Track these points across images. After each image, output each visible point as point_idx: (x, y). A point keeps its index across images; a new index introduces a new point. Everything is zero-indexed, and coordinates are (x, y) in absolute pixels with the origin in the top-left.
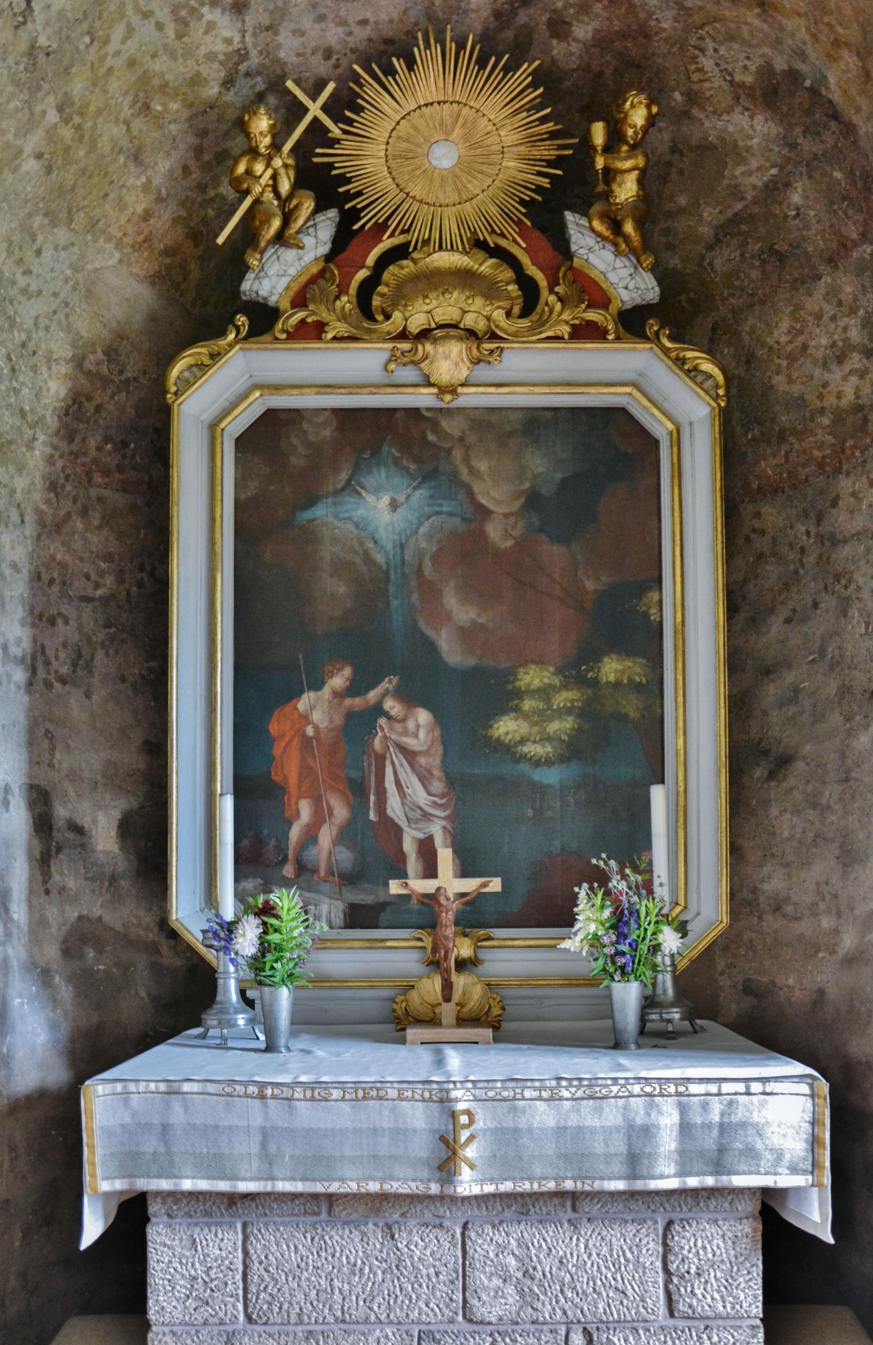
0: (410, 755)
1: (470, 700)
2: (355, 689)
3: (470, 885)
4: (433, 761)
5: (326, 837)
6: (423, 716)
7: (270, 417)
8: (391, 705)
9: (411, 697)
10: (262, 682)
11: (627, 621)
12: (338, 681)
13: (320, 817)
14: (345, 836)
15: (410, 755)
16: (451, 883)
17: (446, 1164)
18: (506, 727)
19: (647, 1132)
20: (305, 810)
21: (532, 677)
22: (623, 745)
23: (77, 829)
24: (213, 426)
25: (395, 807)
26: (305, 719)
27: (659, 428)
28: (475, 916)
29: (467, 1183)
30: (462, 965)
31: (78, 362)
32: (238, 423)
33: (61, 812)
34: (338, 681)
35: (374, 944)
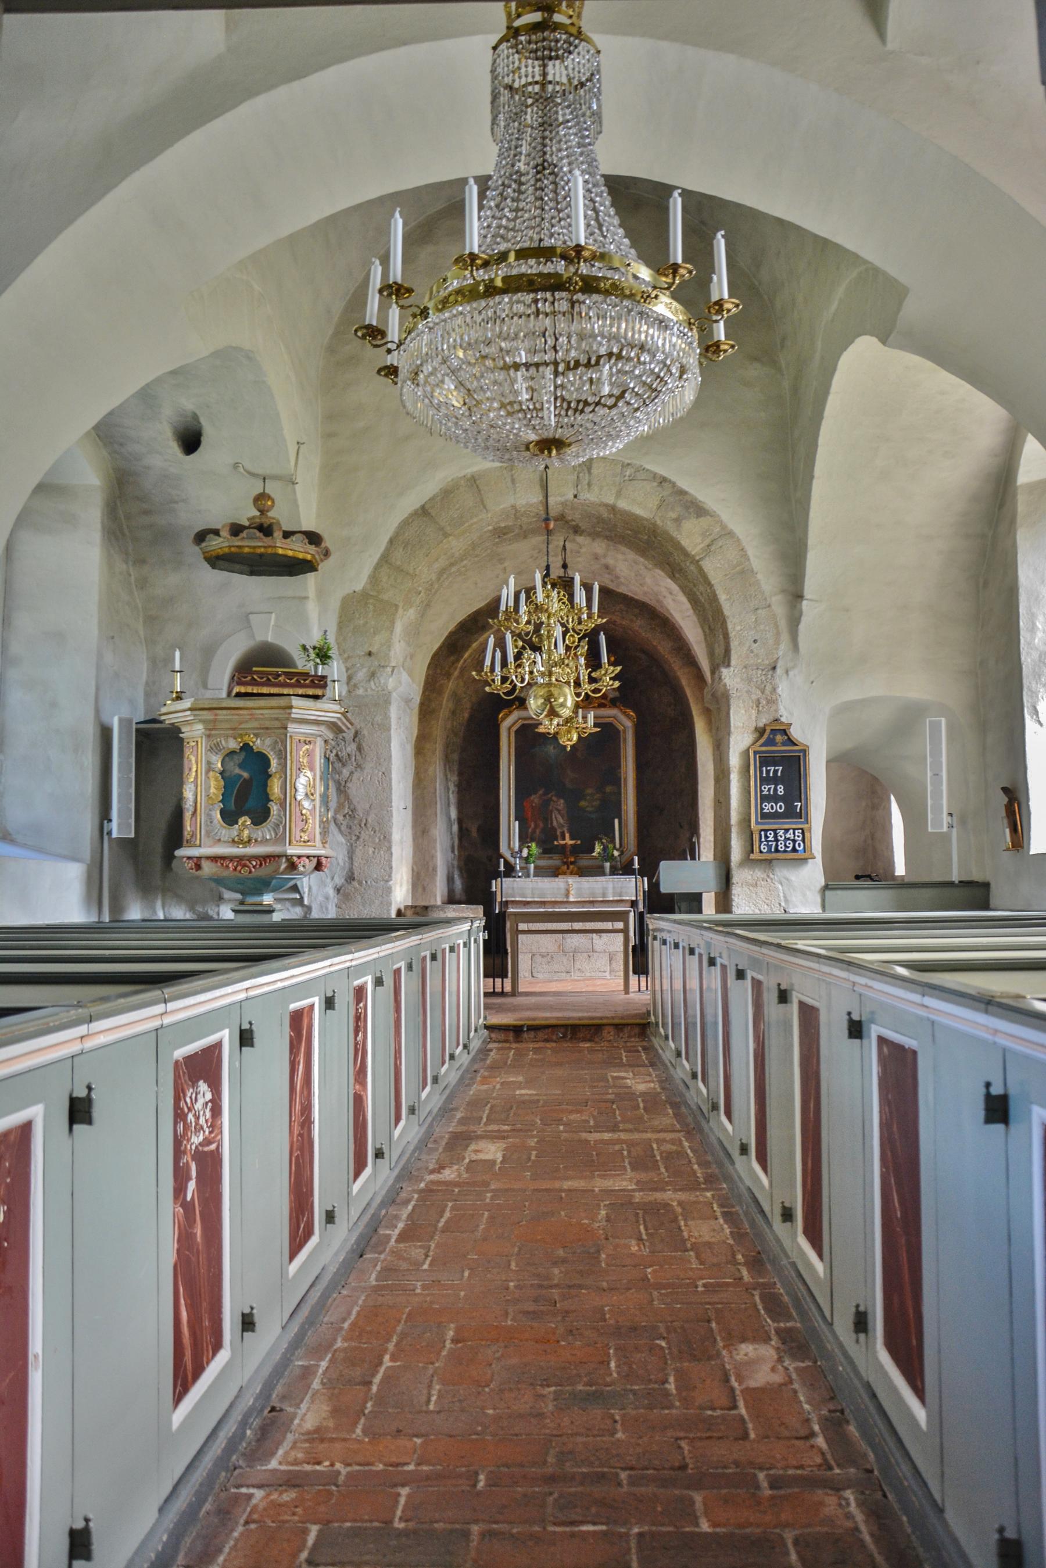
0: (559, 811)
1: (573, 797)
2: (545, 794)
3: (572, 842)
4: (564, 812)
5: (538, 831)
6: (562, 801)
7: (523, 725)
8: (554, 798)
9: (559, 797)
10: (523, 791)
11: (614, 778)
12: (541, 792)
13: (536, 826)
14: (543, 831)
15: (559, 811)
16: (569, 842)
17: (567, 895)
18: (583, 803)
19: (606, 888)
20: (533, 826)
21: (589, 791)
22: (612, 807)
23: (467, 829)
24: (510, 729)
25: (555, 823)
26: (533, 801)
27: (621, 728)
28: (575, 850)
29: (572, 899)
30: (572, 863)
31: (472, 708)
32: (515, 728)
33: (464, 826)
34: (541, 792)
35: (551, 858)
